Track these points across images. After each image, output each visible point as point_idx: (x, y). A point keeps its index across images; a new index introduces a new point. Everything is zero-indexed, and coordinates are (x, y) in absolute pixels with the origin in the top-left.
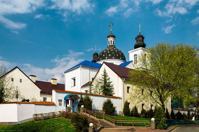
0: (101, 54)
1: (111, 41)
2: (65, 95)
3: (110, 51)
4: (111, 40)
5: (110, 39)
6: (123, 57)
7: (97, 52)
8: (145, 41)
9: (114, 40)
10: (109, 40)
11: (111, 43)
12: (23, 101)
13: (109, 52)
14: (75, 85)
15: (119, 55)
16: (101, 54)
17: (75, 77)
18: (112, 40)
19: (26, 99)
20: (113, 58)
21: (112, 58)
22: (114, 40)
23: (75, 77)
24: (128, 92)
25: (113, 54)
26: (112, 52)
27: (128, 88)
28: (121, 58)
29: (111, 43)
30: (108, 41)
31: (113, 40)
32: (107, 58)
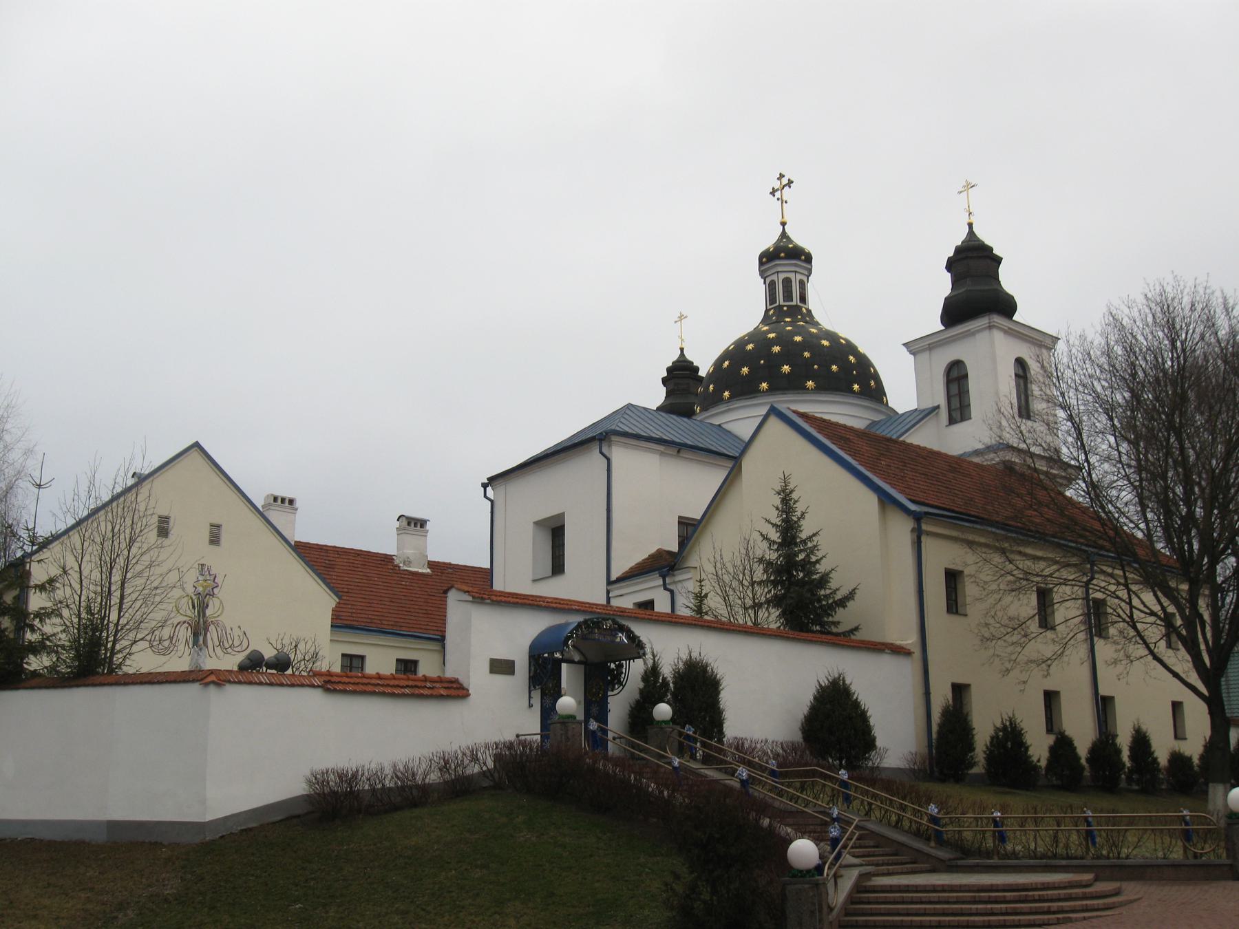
0: (727, 363)
1: (787, 283)
2: (531, 626)
3: (783, 339)
4: (782, 276)
5: (779, 269)
6: (872, 383)
7: (689, 356)
8: (1009, 279)
10: (774, 277)
11: (788, 296)
12: (242, 668)
13: (776, 349)
15: (846, 367)
16: (727, 363)
17: (564, 513)
18: (792, 276)
19: (269, 653)
20: (810, 384)
21: (802, 388)
22: (805, 279)
23: (564, 513)
24: (954, 605)
25: (808, 363)
26: (804, 346)
27: (953, 578)
28: (856, 387)
29: (788, 296)
30: (768, 281)
31: (799, 277)
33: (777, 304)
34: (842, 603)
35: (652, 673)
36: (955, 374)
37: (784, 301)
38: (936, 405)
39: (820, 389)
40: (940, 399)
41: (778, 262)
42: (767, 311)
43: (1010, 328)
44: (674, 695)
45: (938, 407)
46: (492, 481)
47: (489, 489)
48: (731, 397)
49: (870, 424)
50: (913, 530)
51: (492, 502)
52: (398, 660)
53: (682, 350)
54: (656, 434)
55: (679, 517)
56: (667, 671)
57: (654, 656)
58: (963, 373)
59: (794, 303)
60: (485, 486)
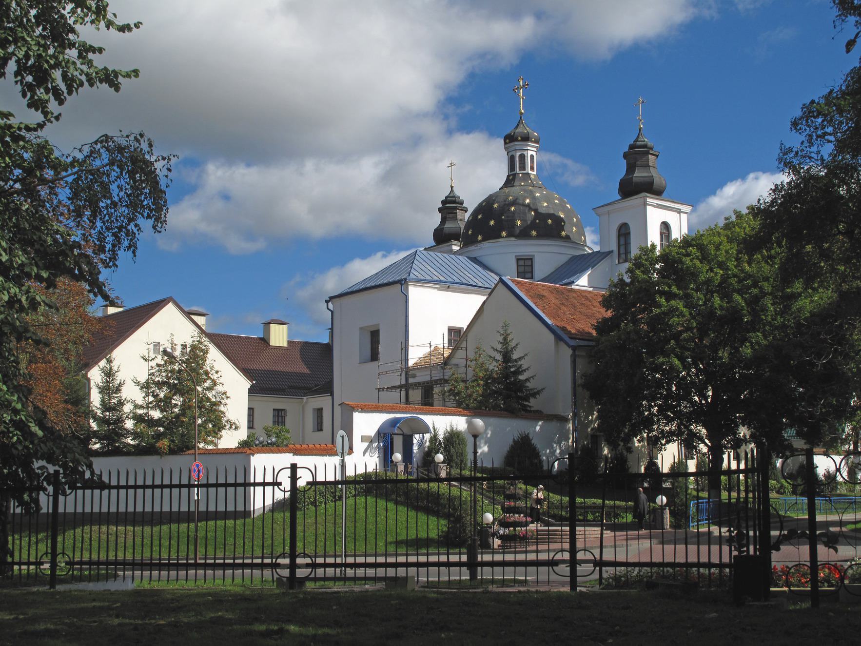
7: (457, 192)
9: (534, 154)
10: (513, 153)
14: (374, 357)
23: (379, 324)
30: (510, 154)
32: (504, 234)
33: (515, 172)
34: (534, 395)
35: (434, 438)
36: (623, 231)
37: (520, 170)
38: (611, 250)
39: (539, 236)
40: (614, 247)
41: (516, 143)
42: (508, 176)
43: (657, 204)
44: (445, 448)
45: (612, 252)
46: (331, 298)
47: (330, 304)
48: (483, 240)
49: (571, 258)
50: (571, 356)
51: (332, 312)
52: (274, 410)
53: (452, 187)
54: (437, 275)
55: (449, 327)
56: (441, 437)
57: (435, 430)
58: (628, 232)
59: (526, 172)
60: (327, 302)
